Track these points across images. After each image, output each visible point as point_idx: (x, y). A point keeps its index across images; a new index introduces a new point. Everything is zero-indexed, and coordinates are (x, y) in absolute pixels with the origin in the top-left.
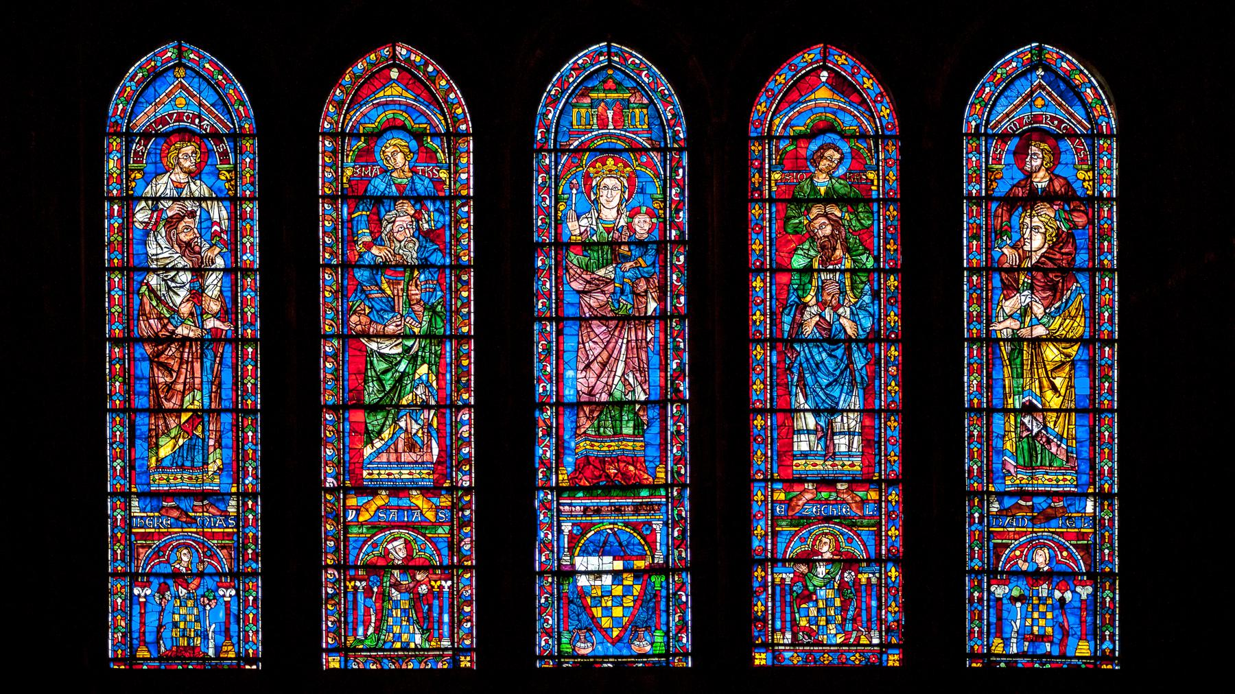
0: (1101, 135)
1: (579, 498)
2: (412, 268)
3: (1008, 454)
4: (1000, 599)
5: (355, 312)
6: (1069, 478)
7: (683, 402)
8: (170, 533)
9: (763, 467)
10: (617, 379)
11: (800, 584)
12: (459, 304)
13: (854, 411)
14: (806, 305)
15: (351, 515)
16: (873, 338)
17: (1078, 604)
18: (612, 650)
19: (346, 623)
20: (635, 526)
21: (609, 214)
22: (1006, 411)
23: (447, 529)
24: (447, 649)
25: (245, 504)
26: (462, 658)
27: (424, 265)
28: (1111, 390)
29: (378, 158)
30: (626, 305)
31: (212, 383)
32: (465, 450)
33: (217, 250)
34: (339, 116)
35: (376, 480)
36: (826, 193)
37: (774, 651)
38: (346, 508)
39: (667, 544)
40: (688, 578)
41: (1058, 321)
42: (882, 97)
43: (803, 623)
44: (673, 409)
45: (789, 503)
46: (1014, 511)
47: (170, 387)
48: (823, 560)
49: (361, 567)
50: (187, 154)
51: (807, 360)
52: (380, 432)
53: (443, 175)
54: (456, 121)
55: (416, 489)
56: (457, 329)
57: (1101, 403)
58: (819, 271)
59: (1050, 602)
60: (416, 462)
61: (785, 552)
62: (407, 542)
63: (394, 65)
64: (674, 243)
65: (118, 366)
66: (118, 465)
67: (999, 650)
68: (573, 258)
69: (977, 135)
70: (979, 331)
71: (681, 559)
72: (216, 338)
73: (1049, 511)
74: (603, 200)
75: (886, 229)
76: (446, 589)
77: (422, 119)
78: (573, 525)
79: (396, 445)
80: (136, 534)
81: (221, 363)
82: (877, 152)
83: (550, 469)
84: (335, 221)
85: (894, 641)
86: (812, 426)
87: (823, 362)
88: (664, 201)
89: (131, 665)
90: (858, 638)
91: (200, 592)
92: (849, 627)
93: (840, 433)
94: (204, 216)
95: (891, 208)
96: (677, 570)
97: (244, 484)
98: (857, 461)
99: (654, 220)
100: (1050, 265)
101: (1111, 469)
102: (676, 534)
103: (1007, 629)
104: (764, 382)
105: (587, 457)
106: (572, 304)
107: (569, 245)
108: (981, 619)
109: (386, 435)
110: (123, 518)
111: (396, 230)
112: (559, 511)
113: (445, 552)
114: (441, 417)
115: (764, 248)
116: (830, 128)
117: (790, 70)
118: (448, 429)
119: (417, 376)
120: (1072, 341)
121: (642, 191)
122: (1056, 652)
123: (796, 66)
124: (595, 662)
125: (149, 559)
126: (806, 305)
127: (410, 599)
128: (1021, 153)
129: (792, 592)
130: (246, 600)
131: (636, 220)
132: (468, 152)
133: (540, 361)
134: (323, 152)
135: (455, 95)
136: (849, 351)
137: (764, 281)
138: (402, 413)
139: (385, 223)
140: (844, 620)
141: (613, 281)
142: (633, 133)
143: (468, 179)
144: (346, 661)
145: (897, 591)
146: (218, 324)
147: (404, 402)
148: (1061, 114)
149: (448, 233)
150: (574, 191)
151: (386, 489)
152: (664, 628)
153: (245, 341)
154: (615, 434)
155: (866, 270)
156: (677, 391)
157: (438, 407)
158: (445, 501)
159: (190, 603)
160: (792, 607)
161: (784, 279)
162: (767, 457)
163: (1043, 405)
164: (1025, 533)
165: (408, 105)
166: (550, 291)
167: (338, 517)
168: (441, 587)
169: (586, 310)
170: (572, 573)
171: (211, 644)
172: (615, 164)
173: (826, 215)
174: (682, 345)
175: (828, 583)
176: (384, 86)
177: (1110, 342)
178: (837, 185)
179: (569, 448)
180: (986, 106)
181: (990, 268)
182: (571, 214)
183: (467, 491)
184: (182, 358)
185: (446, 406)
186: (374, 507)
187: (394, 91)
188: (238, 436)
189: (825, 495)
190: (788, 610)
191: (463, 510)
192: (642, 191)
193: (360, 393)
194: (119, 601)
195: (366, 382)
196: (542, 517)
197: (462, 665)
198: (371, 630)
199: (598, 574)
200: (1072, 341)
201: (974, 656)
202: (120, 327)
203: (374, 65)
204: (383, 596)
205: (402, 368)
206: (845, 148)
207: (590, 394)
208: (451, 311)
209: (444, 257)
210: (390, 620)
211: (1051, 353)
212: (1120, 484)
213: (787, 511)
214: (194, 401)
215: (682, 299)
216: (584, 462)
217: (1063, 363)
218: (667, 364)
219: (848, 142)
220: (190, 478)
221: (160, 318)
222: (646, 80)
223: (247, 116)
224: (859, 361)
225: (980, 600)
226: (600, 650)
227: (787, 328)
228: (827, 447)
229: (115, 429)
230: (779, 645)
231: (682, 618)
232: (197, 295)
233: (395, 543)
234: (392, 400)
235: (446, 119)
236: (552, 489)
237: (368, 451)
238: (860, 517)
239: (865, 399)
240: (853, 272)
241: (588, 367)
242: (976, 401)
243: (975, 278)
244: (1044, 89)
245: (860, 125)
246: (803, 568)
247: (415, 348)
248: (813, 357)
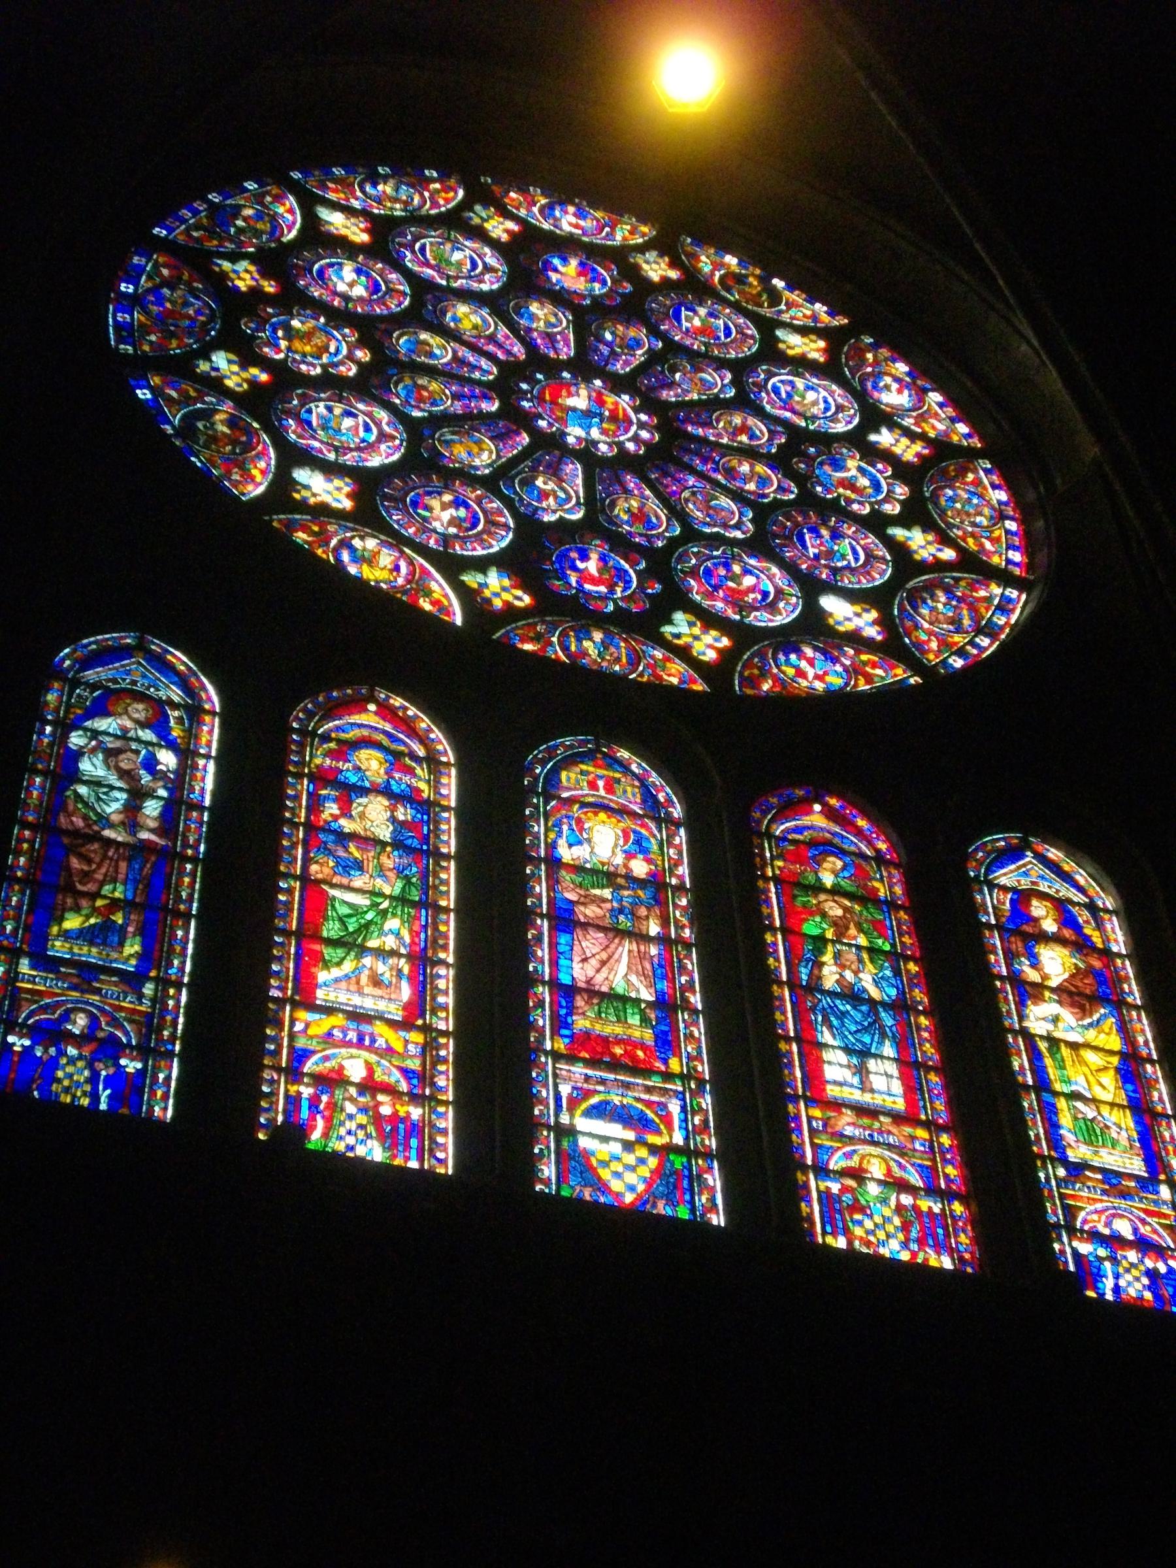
2: (384, 844)
5: (316, 862)
25: (165, 991)
58: (833, 942)
78: (574, 1088)
126: (823, 964)
146: (153, 837)
159: (80, 1064)
176: (360, 712)
205: (370, 916)
207: (588, 982)
227: (804, 977)
228: (862, 1082)
246: (851, 1183)
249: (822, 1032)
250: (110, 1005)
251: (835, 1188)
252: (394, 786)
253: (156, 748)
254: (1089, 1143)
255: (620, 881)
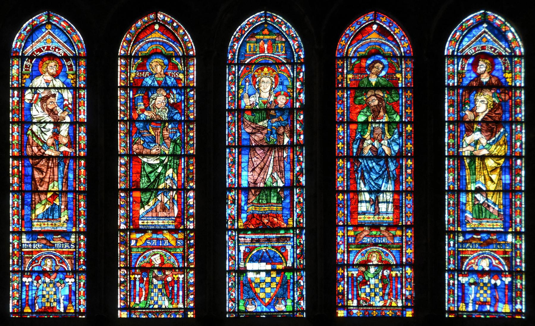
0: (515, 56)
1: (249, 234)
2: (165, 122)
3: (468, 212)
4: (464, 284)
5: (136, 143)
6: (499, 224)
7: (301, 187)
8: (41, 251)
9: (342, 219)
10: (268, 176)
11: (361, 277)
12: (189, 139)
13: (389, 191)
14: (365, 139)
15: (133, 243)
16: (399, 156)
17: (503, 287)
18: (265, 309)
19: (130, 295)
20: (277, 248)
21: (265, 95)
22: (467, 192)
23: (182, 249)
24: (181, 308)
25: (79, 237)
26: (189, 313)
27: (171, 120)
28: (521, 181)
29: (148, 68)
30: (273, 139)
31: (63, 178)
32: (191, 211)
33: (67, 113)
34: (129, 47)
35: (146, 225)
36: (376, 84)
37: (348, 310)
38: (130, 240)
39: (293, 257)
40: (304, 274)
41: (494, 147)
42: (405, 37)
43: (363, 295)
44: (297, 191)
45: (355, 237)
46: (471, 241)
47: (42, 180)
48: (373, 265)
49: (138, 268)
50: (52, 67)
51: (365, 166)
52: (148, 202)
53: (181, 76)
54: (188, 49)
55: (166, 230)
56: (188, 151)
57: (515, 187)
58: (372, 123)
59: (489, 285)
60: (166, 217)
61: (354, 261)
62: (161, 256)
63: (157, 23)
64: (298, 110)
65: (16, 170)
66: (16, 218)
67: (464, 309)
68: (247, 116)
69: (452, 56)
70: (453, 152)
71: (300, 264)
72: (65, 157)
73: (489, 240)
74: (261, 88)
75: (406, 102)
76: (181, 279)
77: (171, 49)
78: (246, 247)
79: (156, 208)
80: (24, 252)
81: (68, 169)
82: (402, 64)
83: (234, 220)
84: (126, 99)
85: (409, 304)
86: (368, 199)
87: (373, 167)
88: (293, 89)
89: (21, 315)
90: (391, 303)
91: (57, 279)
92: (386, 298)
93: (382, 202)
94: (60, 97)
95: (409, 92)
96: (298, 270)
97: (79, 228)
98: (391, 216)
99: (288, 98)
100: (490, 119)
101: (521, 220)
102: (298, 252)
103: (467, 299)
104: (343, 177)
105: (253, 214)
106: (246, 139)
107: (245, 110)
108: (454, 294)
109: (151, 203)
110: (18, 244)
111: (156, 103)
112: (239, 241)
113: (181, 260)
114: (178, 193)
115: (344, 112)
116: (377, 52)
117: (357, 24)
118: (182, 201)
119: (167, 175)
120: (500, 157)
121: (282, 84)
122: (492, 310)
123: (360, 22)
124: (256, 315)
125: (31, 264)
126: (365, 139)
127: (162, 284)
128: (475, 65)
129: (357, 280)
130: (79, 284)
131: (279, 98)
132: (194, 65)
133: (229, 167)
134: (120, 66)
135: (188, 37)
136: (387, 163)
137: (343, 128)
138: (159, 193)
139: (151, 100)
140: (384, 294)
141: (267, 128)
142: (277, 55)
143: (193, 78)
144: (130, 314)
145: (411, 280)
146: (66, 149)
147: (160, 187)
148: (496, 46)
149: (183, 105)
150: (247, 84)
151: (151, 230)
152: (292, 298)
153: (80, 158)
154: (267, 203)
155: (396, 122)
156: (299, 181)
157: (177, 190)
158: (180, 236)
159: (51, 285)
160: (357, 288)
161: (353, 127)
162: (344, 214)
163: (486, 188)
164: (477, 251)
165: (163, 42)
166: (235, 133)
167: (125, 243)
168: (178, 278)
169: (253, 142)
170: (245, 271)
171: (62, 305)
172: (268, 71)
173: (375, 95)
174: (301, 159)
175: (376, 276)
176: (151, 33)
177: (520, 157)
178: (381, 81)
179: (244, 210)
180: (457, 42)
181: (460, 121)
182: (246, 95)
183: (191, 231)
184: (48, 166)
185: (182, 190)
186: (144, 239)
187: (156, 36)
188: (76, 204)
189: (374, 233)
190: (355, 289)
191: (190, 240)
192: (282, 84)
193: (138, 183)
194: (16, 284)
195: (141, 177)
196: (230, 243)
197: (189, 316)
198: (143, 299)
199: (258, 272)
200: (500, 157)
201: (450, 312)
202: (17, 150)
203: (147, 22)
204: (149, 282)
205: (159, 170)
206: (385, 62)
207: (255, 183)
208: (184, 143)
209: (181, 116)
210: (152, 294)
211: (490, 163)
212: (525, 227)
213: (355, 240)
214: (56, 186)
215: (302, 137)
216: (251, 217)
217: (496, 168)
218: (294, 169)
219: (387, 59)
220: (52, 224)
221: (38, 146)
222: (284, 29)
223: (82, 48)
224: (392, 167)
225: (454, 284)
226: (259, 309)
227: (355, 150)
228: (375, 209)
229: (14, 201)
230: (350, 306)
231: (301, 293)
232: (56, 134)
233: (155, 257)
234: (154, 186)
235: (182, 49)
236: (235, 230)
237: (142, 211)
238: (392, 244)
239: (395, 186)
240: (389, 123)
241: (253, 170)
242: (451, 186)
243: (451, 126)
244: (487, 33)
245: (393, 51)
246: (363, 269)
247: (166, 161)
248: (368, 165)
249: (360, 183)
250: (59, 252)
251: (355, 273)
252: (169, 82)
253: (62, 86)
254: (478, 218)
255: (272, 112)
